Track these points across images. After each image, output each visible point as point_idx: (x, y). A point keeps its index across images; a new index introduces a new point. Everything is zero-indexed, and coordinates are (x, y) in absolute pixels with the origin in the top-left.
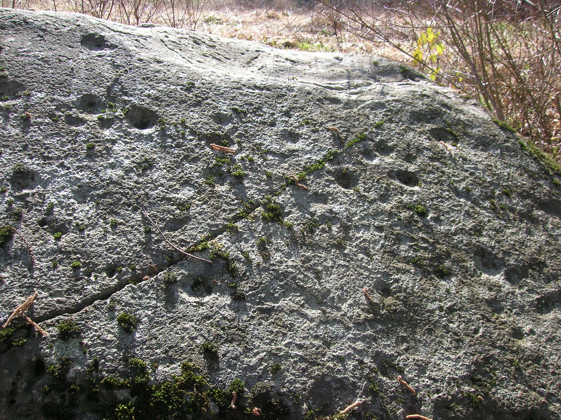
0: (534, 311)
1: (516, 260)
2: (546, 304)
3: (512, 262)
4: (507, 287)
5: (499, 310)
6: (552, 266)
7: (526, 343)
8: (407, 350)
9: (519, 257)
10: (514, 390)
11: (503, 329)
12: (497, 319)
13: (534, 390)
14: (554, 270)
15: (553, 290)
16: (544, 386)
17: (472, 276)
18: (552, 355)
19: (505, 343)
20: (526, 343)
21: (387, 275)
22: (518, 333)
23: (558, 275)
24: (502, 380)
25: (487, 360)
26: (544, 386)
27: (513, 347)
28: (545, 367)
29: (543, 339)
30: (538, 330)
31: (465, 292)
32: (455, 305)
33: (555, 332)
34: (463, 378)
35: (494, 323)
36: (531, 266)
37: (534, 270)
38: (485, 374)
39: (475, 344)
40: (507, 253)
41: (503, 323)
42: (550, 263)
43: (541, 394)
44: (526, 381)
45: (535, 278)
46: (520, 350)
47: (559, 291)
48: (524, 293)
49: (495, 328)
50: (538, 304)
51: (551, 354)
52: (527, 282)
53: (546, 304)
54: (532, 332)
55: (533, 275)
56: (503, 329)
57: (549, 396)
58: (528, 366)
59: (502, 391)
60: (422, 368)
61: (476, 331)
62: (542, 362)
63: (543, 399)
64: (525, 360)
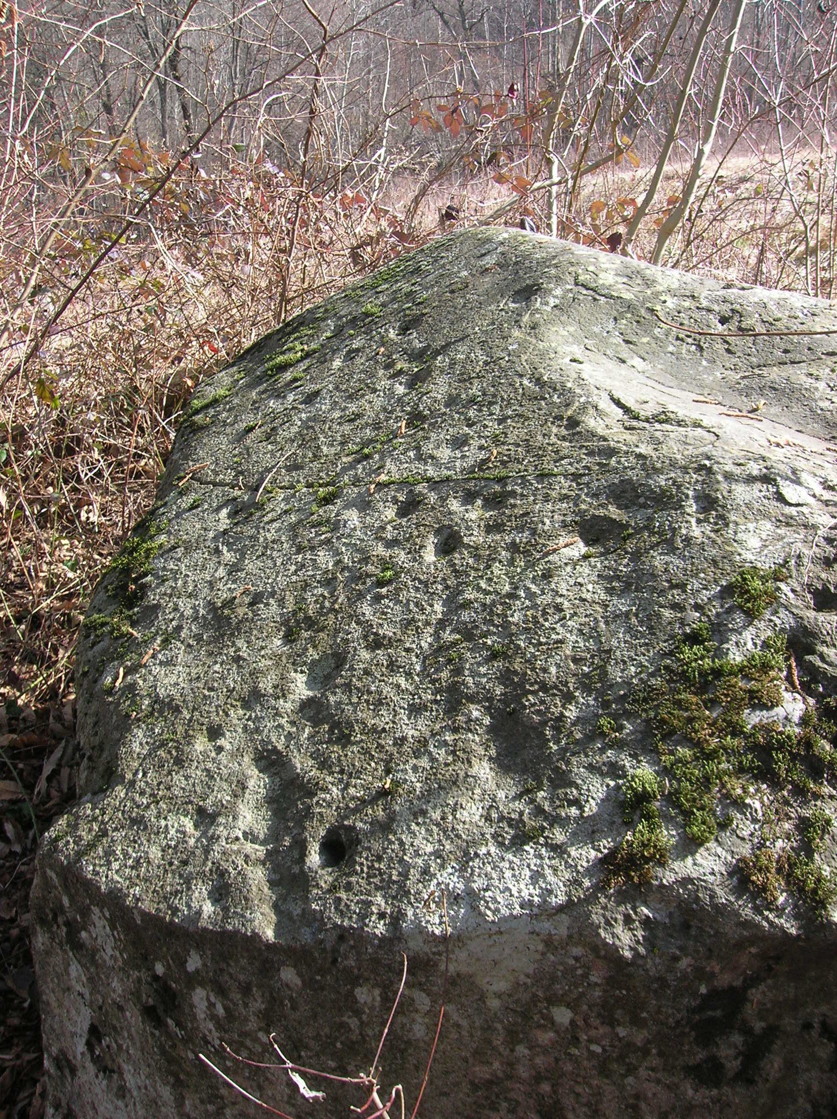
0: (257, 749)
1: (339, 703)
2: (273, 764)
3: (332, 699)
4: (287, 706)
5: (246, 705)
6: (346, 755)
7: (201, 744)
8: (189, 646)
9: (347, 704)
10: (141, 744)
11: (218, 714)
12: (232, 706)
13: (141, 765)
14: (339, 761)
15: (298, 765)
16: (145, 774)
17: (293, 664)
18: (186, 779)
19: (198, 720)
20: (201, 744)
21: (273, 594)
22: (214, 733)
23: (330, 767)
24: (153, 729)
25: (177, 710)
26: (145, 774)
27: (194, 730)
28: (169, 773)
29: (209, 765)
30: (223, 757)
31: (264, 663)
32: (245, 660)
33: (221, 779)
34: (157, 695)
35: (226, 703)
36: (335, 725)
37: (331, 731)
38: (161, 712)
39: (194, 693)
40: (348, 687)
41: (227, 715)
42: (353, 752)
43: (135, 774)
44: (150, 754)
45: (313, 736)
46: (188, 738)
47: (298, 774)
48: (284, 730)
49: (217, 707)
50: (267, 751)
51: (187, 778)
52: (303, 729)
53: (273, 764)
54: (220, 749)
55: (318, 732)
56: (218, 714)
57: (132, 783)
58: (170, 752)
59: (140, 734)
60: (169, 663)
61: (211, 689)
62: (176, 768)
63: (129, 776)
64: (177, 748)
